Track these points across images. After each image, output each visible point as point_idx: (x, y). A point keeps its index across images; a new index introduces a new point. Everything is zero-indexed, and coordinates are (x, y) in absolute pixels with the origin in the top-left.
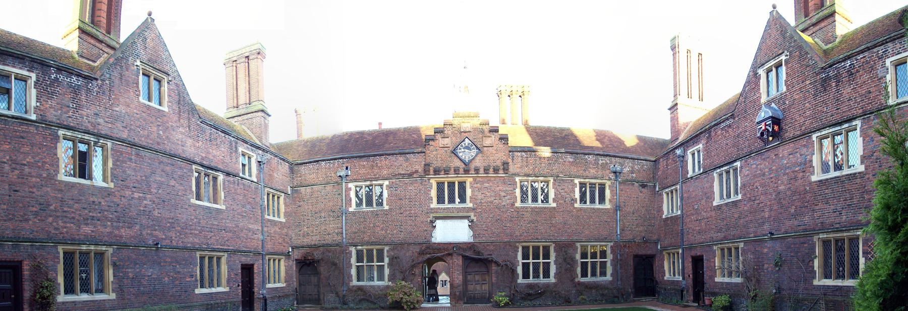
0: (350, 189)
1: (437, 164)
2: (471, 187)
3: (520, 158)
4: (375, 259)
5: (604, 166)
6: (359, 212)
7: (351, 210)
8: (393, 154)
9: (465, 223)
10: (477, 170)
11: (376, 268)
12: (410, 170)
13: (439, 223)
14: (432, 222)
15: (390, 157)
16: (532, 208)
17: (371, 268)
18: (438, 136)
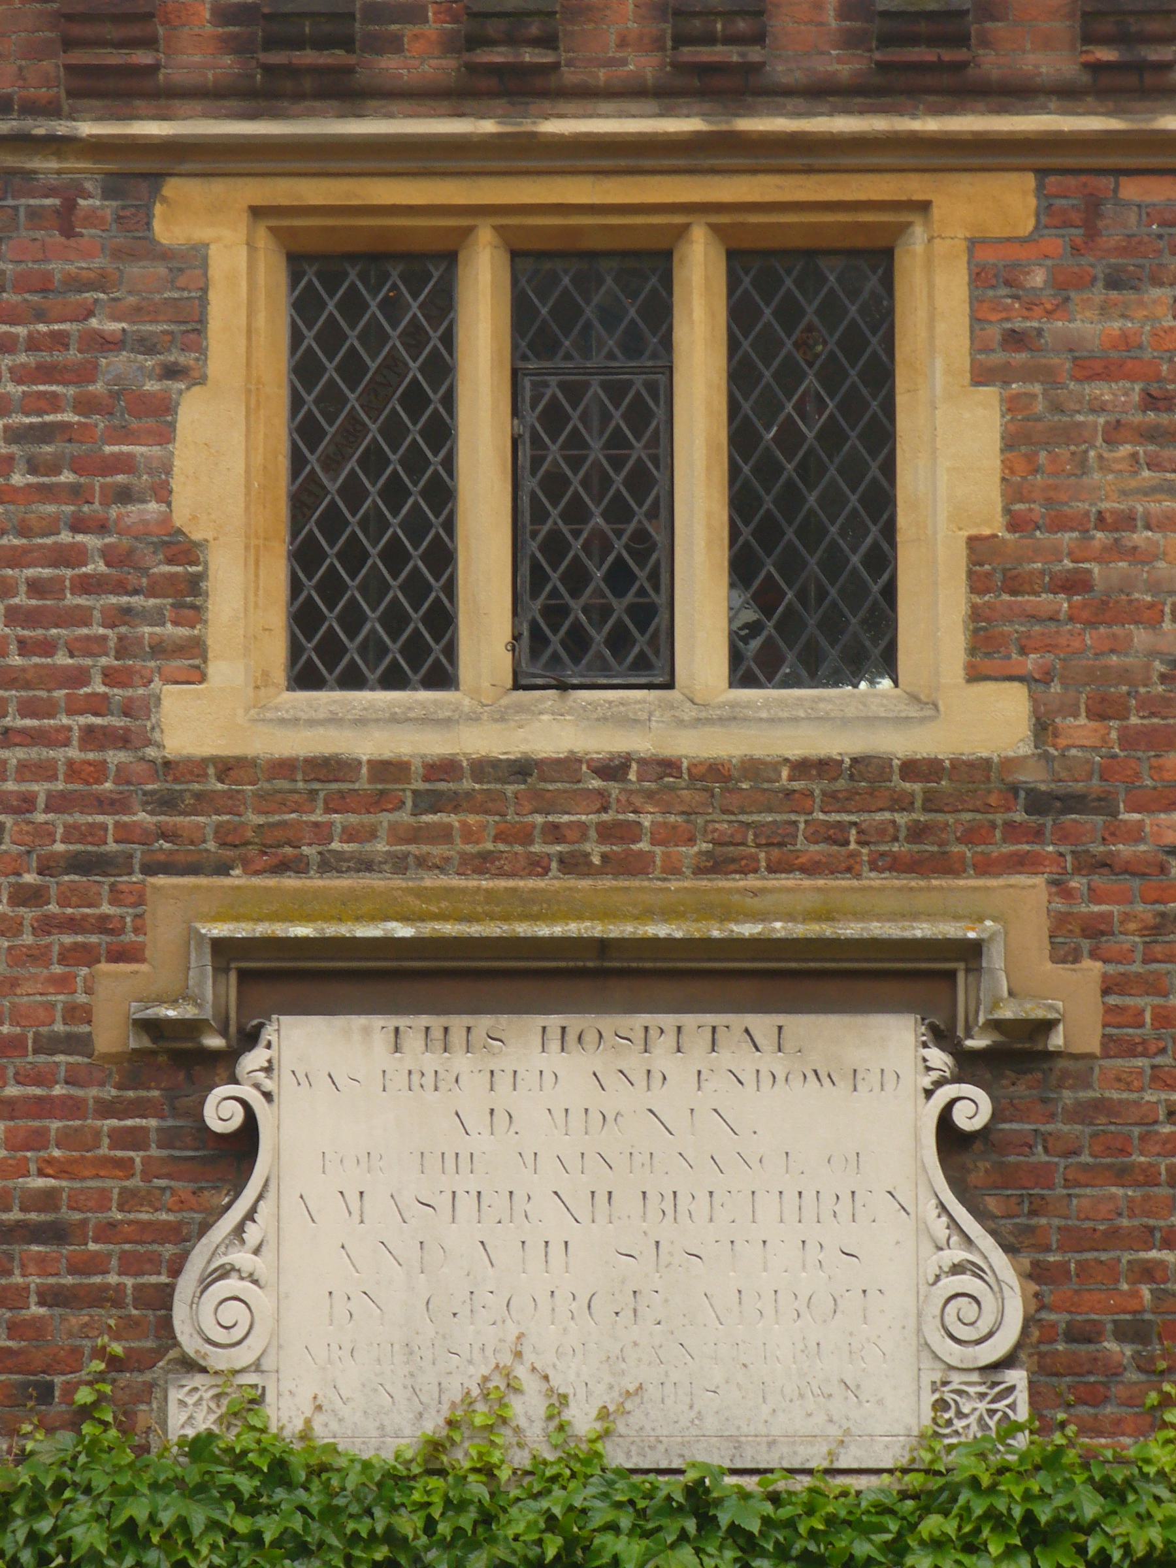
2: (1005, 353)
9: (879, 1091)
13: (327, 1092)
14: (182, 1059)
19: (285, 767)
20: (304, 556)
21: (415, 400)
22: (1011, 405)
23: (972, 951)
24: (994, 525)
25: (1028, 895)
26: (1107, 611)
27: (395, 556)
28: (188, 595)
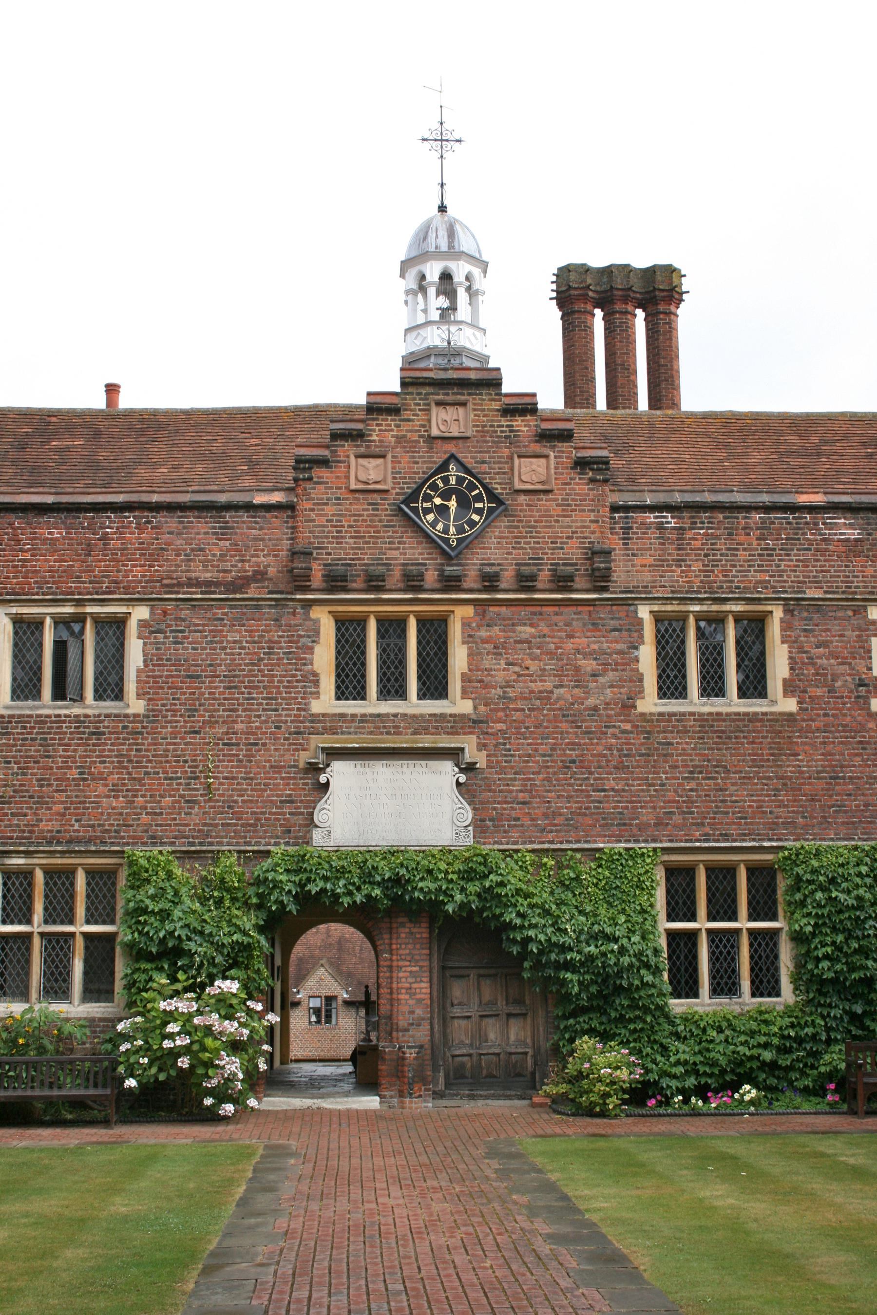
1: (342, 550)
2: (469, 638)
3: (653, 534)
4: (80, 910)
6: (22, 720)
8: (171, 508)
9: (446, 773)
10: (490, 582)
11: (80, 943)
12: (234, 568)
14: (314, 769)
16: (703, 720)
17: (58, 945)
18: (347, 449)
19: (334, 715)
20: (338, 676)
21: (359, 647)
22: (469, 648)
23: (462, 750)
24: (466, 670)
25: (474, 738)
26: (487, 686)
27: (355, 676)
28: (316, 683)
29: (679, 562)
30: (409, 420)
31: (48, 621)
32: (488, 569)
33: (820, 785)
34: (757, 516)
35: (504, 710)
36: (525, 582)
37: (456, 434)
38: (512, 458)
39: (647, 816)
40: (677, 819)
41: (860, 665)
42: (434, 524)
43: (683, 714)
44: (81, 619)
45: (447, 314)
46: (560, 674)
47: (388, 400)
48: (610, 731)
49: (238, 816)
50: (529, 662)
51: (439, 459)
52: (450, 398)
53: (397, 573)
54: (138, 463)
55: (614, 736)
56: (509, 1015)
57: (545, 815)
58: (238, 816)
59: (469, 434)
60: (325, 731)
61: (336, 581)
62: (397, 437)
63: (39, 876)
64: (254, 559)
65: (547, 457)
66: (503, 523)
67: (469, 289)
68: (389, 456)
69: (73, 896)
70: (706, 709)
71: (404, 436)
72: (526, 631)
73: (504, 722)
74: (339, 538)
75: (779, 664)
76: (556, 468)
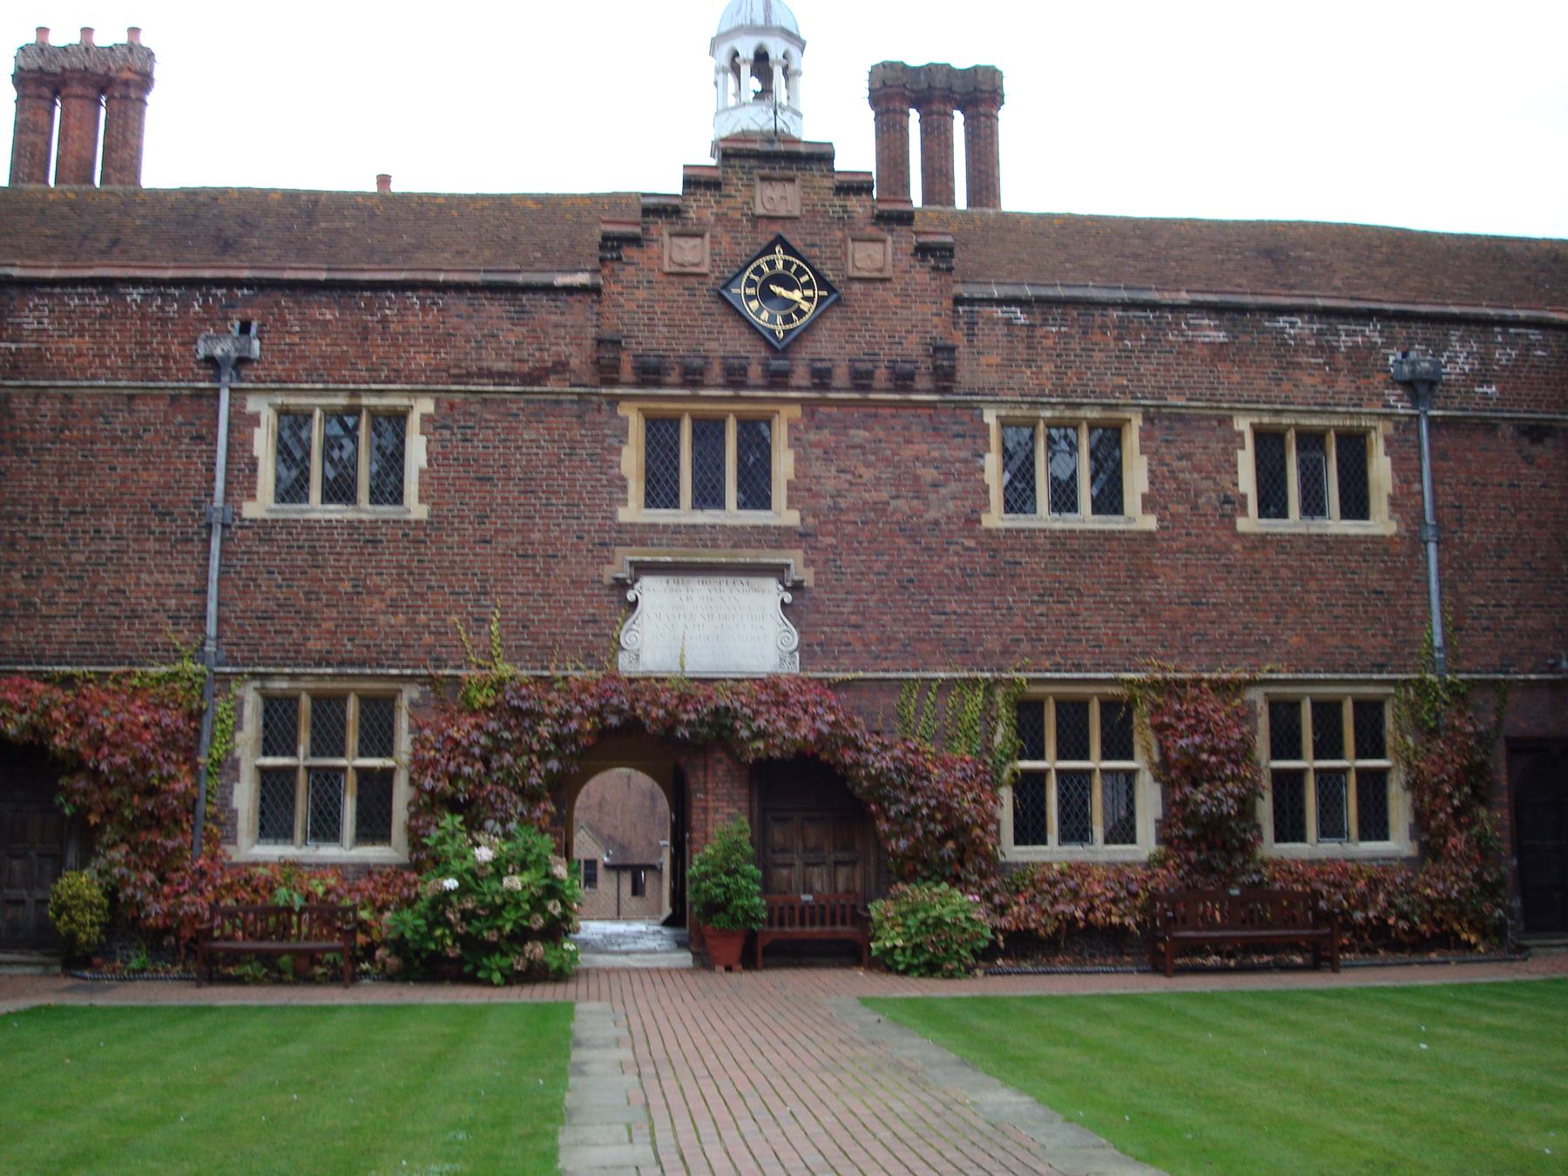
0: (255, 420)
1: (652, 340)
2: (795, 442)
3: (1001, 330)
4: (352, 741)
5: (1361, 361)
6: (287, 525)
7: (251, 510)
8: (460, 288)
9: (770, 594)
10: (821, 378)
11: (351, 782)
13: (652, 593)
14: (622, 586)
15: (449, 299)
17: (326, 782)
18: (661, 228)
19: (644, 525)
20: (648, 481)
21: (671, 449)
22: (797, 454)
23: (788, 566)
24: (792, 477)
25: (799, 553)
26: (815, 495)
27: (667, 482)
28: (624, 489)
29: (1029, 362)
30: (730, 196)
31: (318, 413)
32: (819, 365)
33: (1182, 611)
34: (1115, 314)
35: (834, 522)
36: (861, 380)
37: (783, 213)
38: (844, 241)
39: (992, 643)
40: (1025, 646)
41: (1225, 480)
42: (758, 313)
43: (1032, 531)
44: (355, 411)
45: (765, 93)
46: (897, 483)
47: (707, 173)
48: (952, 548)
49: (534, 637)
50: (862, 470)
51: (764, 240)
52: (777, 173)
53: (716, 369)
54: (418, 248)
55: (957, 554)
56: (837, 863)
57: (880, 641)
58: (534, 637)
59: (797, 213)
60: (633, 542)
61: (650, 374)
62: (717, 215)
63: (305, 703)
64: (554, 348)
65: (884, 241)
66: (836, 314)
67: (785, 70)
68: (707, 236)
69: (343, 726)
70: (1058, 526)
71: (725, 214)
72: (860, 435)
73: (835, 536)
74: (651, 326)
75: (1136, 478)
76: (894, 254)
